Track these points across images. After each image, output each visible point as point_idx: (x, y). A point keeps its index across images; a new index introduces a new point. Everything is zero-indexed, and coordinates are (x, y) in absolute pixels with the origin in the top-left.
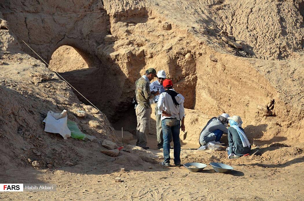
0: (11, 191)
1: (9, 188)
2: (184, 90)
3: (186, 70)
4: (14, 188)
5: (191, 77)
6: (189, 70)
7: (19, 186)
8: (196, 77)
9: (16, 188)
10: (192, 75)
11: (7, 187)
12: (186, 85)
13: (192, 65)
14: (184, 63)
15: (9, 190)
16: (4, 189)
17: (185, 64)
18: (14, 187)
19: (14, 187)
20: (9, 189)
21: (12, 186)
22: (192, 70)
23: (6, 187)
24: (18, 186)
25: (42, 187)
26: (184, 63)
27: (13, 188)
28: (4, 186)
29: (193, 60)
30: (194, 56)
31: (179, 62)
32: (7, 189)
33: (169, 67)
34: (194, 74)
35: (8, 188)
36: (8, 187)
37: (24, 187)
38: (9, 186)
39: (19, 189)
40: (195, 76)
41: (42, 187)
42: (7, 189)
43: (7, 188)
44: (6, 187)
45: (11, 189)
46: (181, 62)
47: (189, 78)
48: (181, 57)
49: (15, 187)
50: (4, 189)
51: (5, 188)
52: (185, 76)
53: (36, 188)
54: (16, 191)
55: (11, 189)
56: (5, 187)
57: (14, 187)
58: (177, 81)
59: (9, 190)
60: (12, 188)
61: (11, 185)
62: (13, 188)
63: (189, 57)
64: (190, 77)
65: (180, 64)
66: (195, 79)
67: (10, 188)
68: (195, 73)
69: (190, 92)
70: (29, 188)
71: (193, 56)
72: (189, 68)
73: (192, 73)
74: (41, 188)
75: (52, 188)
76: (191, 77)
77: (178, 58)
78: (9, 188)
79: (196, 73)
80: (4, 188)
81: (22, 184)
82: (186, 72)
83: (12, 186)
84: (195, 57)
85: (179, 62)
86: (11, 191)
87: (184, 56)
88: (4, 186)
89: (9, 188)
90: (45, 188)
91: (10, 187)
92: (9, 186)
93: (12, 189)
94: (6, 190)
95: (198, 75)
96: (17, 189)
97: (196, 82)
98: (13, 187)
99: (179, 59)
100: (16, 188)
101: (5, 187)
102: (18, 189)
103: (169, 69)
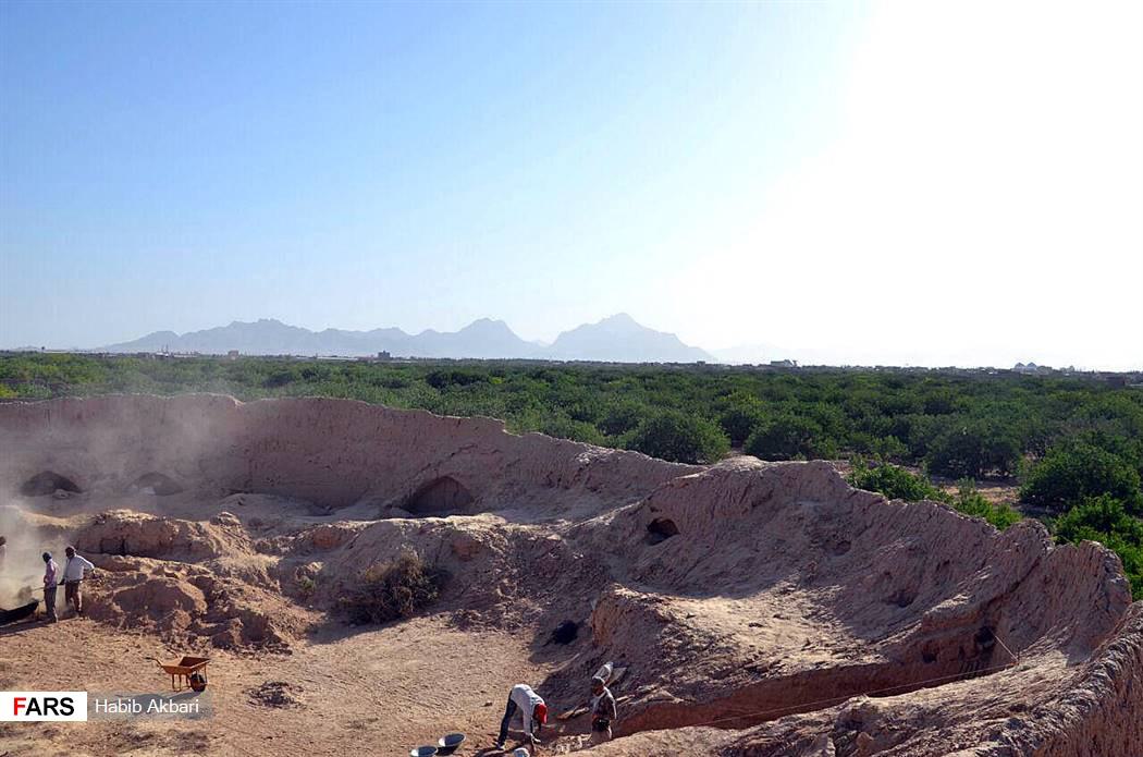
0: (42, 718)
1: (34, 707)
4: (52, 707)
7: (71, 701)
9: (59, 707)
11: (27, 703)
16: (16, 713)
18: (52, 703)
19: (52, 703)
20: (34, 710)
21: (46, 700)
23: (23, 706)
24: (67, 702)
25: (158, 706)
27: (49, 709)
28: (16, 700)
32: (28, 713)
35: (30, 709)
36: (31, 704)
37: (90, 708)
38: (34, 700)
39: (72, 710)
41: (158, 706)
42: (28, 713)
43: (26, 709)
44: (23, 706)
45: (40, 714)
49: (56, 704)
50: (16, 713)
51: (19, 710)
53: (137, 708)
54: (62, 718)
55: (40, 714)
56: (19, 703)
57: (51, 703)
59: (34, 716)
60: (46, 707)
61: (40, 696)
62: (49, 709)
67: (37, 709)
74: (156, 707)
78: (33, 706)
80: (16, 706)
81: (84, 695)
83: (46, 700)
86: (42, 718)
88: (16, 700)
89: (34, 707)
91: (37, 705)
92: (34, 700)
93: (46, 713)
94: (22, 716)
96: (62, 712)
98: (50, 705)
100: (59, 707)
101: (19, 703)
102: (67, 710)
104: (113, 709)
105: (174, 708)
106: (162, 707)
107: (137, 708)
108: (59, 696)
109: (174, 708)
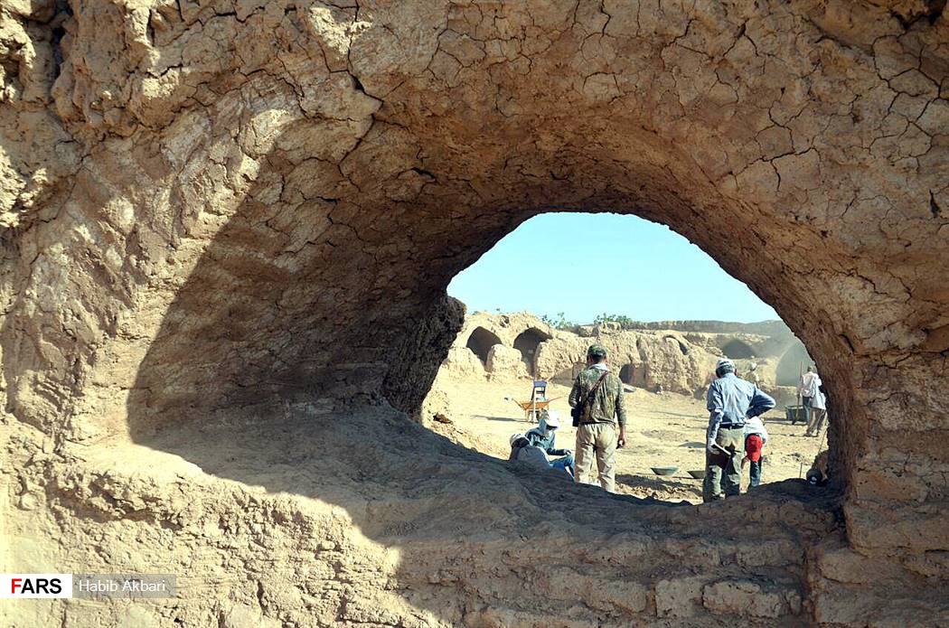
1: (28, 586)
4: (43, 587)
7: (59, 582)
9: (49, 587)
11: (22, 584)
15: (28, 592)
16: (13, 591)
18: (43, 583)
19: (43, 583)
20: (28, 589)
21: (38, 581)
23: (19, 586)
24: (55, 583)
27: (41, 588)
28: (13, 581)
32: (23, 592)
35: (25, 589)
36: (26, 584)
38: (28, 581)
39: (60, 589)
42: (23, 592)
43: (21, 588)
44: (19, 586)
45: (33, 592)
49: (47, 584)
50: (13, 591)
51: (16, 589)
53: (114, 587)
54: (51, 596)
55: (33, 592)
56: (16, 583)
57: (42, 583)
60: (38, 586)
62: (41, 588)
67: (31, 589)
75: (161, 588)
80: (14, 586)
83: (38, 581)
88: (13, 581)
89: (28, 586)
91: (30, 585)
92: (28, 581)
93: (38, 592)
96: (52, 590)
100: (49, 587)
101: (16, 583)
102: (56, 589)
107: (114, 587)
109: (145, 587)
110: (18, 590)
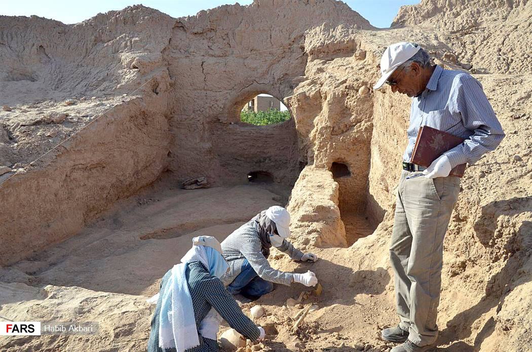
1: (16, 329)
2: (352, 147)
3: (357, 114)
4: (24, 329)
5: (364, 125)
6: (361, 114)
7: (33, 326)
8: (372, 125)
9: (27, 329)
10: (366, 122)
11: (13, 327)
12: (356, 139)
13: (366, 106)
14: (354, 102)
15: (16, 332)
16: (7, 332)
17: (356, 103)
18: (24, 327)
19: (24, 327)
20: (16, 330)
21: (21, 325)
22: (367, 114)
23: (11, 328)
24: (31, 327)
25: (74, 327)
26: (354, 102)
27: (23, 330)
28: (8, 325)
29: (369, 97)
30: (371, 89)
31: (347, 102)
32: (13, 332)
33: (330, 109)
34: (369, 121)
35: (14, 330)
36: (14, 328)
37: (42, 326)
38: (16, 326)
39: (34, 330)
40: (369, 123)
41: (74, 327)
42: (13, 332)
43: (12, 330)
44: (11, 328)
45: (18, 332)
46: (351, 102)
47: (360, 126)
48: (352, 93)
49: (26, 328)
50: (7, 332)
51: (9, 330)
52: (354, 124)
55: (18, 332)
56: (9, 327)
57: (24, 327)
58: (343, 132)
59: (16, 333)
60: (21, 329)
62: (23, 330)
63: (363, 92)
64: (362, 124)
65: (349, 104)
66: (370, 129)
67: (17, 330)
68: (372, 118)
69: (363, 149)
70: (50, 329)
71: (369, 90)
72: (361, 111)
73: (366, 118)
74: (73, 329)
76: (364, 125)
77: (347, 94)
79: (373, 119)
80: (8, 329)
82: (356, 117)
83: (21, 325)
84: (372, 92)
85: (347, 102)
86: (20, 334)
87: (357, 91)
88: (8, 325)
89: (16, 329)
90: (78, 329)
91: (17, 328)
92: (16, 326)
93: (21, 332)
94: (10, 333)
95: (374, 122)
96: (29, 331)
97: (371, 134)
99: (348, 97)
100: (27, 329)
101: (9, 327)
102: (31, 330)
103: (329, 112)
104: (86, 330)
105: (81, 329)
106: (75, 329)
108: (27, 324)
109: (81, 329)
110: (10, 331)
